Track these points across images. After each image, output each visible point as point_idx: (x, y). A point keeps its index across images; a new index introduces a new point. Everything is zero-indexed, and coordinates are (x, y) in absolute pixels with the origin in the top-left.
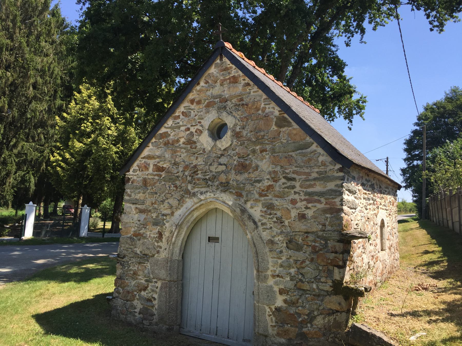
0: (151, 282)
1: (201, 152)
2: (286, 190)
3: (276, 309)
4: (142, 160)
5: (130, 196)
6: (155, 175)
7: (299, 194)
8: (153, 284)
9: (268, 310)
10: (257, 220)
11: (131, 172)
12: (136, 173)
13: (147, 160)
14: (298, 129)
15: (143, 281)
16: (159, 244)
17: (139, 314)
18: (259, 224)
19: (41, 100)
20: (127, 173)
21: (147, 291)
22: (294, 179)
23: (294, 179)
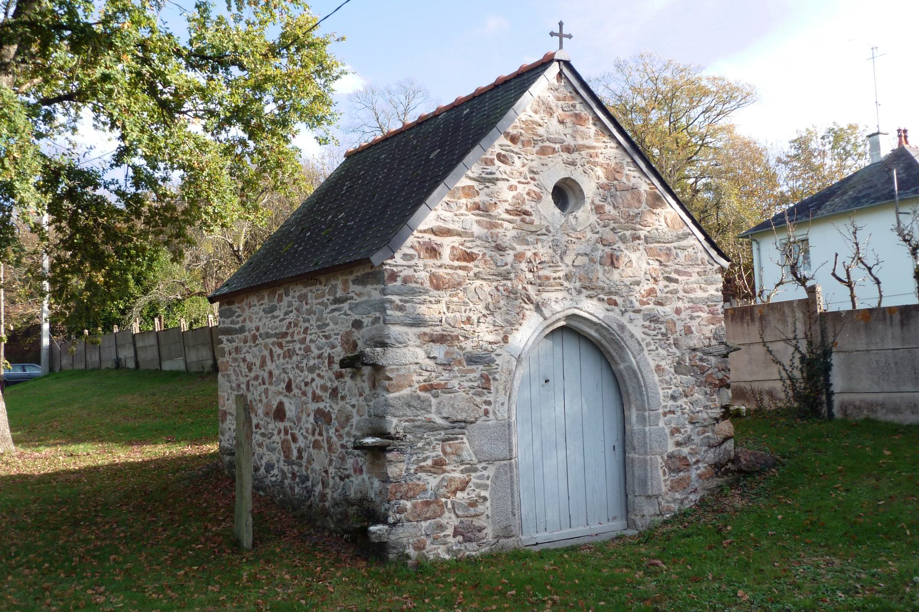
0: (476, 470)
1: (544, 231)
2: (669, 295)
3: (669, 457)
4: (420, 235)
5: (400, 308)
6: (456, 268)
7: (683, 300)
8: (479, 473)
9: (660, 461)
10: (640, 340)
11: (398, 258)
12: (412, 263)
13: (433, 237)
14: (830, 162)
15: (457, 475)
16: (485, 398)
17: (454, 536)
18: (644, 344)
19: (183, 213)
20: (389, 261)
21: (467, 491)
22: (676, 281)
23: (676, 281)
